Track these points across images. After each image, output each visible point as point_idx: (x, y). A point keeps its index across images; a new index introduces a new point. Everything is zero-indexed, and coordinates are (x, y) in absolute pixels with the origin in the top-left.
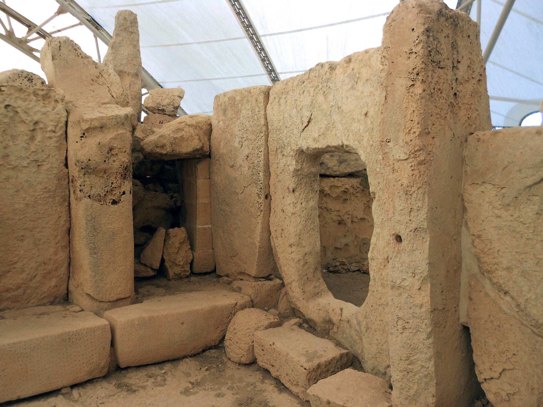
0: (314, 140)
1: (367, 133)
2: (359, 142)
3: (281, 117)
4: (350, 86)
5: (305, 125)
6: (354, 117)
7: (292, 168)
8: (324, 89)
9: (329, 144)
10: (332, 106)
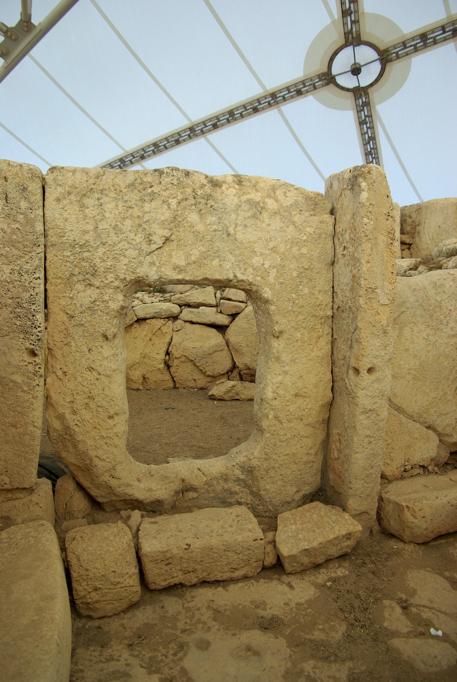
0: (176, 268)
1: (275, 270)
2: (262, 278)
3: (90, 227)
4: (249, 214)
5: (154, 247)
6: (255, 250)
7: (114, 306)
8: (200, 206)
9: (209, 277)
10: (215, 230)
